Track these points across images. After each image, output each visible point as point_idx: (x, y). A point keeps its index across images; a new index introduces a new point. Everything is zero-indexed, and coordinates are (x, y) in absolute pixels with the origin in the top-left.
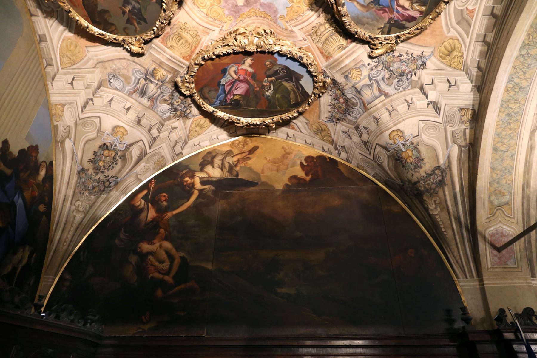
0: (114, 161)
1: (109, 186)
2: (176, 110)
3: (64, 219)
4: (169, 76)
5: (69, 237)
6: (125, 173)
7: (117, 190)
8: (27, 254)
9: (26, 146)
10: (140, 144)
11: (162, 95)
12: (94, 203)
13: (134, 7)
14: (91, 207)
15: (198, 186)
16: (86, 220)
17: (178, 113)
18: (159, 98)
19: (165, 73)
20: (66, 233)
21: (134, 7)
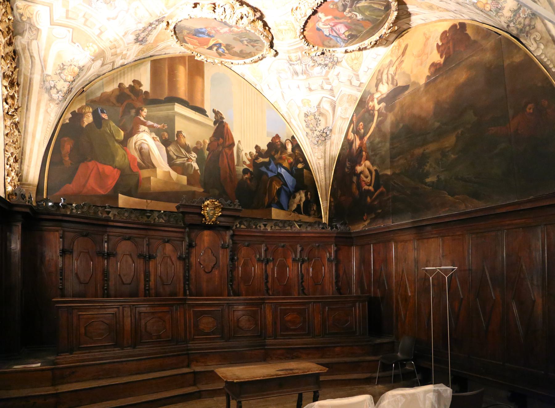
0: (317, 121)
1: (327, 135)
2: (326, 65)
3: (316, 166)
4: (299, 53)
5: (323, 176)
6: (331, 121)
7: (335, 134)
8: (303, 195)
9: (269, 140)
10: (324, 99)
11: (307, 66)
12: (325, 150)
13: (246, 40)
14: (325, 153)
15: (377, 107)
16: (327, 162)
17: (330, 65)
18: (308, 68)
19: (295, 54)
20: (320, 174)
21: (246, 40)
